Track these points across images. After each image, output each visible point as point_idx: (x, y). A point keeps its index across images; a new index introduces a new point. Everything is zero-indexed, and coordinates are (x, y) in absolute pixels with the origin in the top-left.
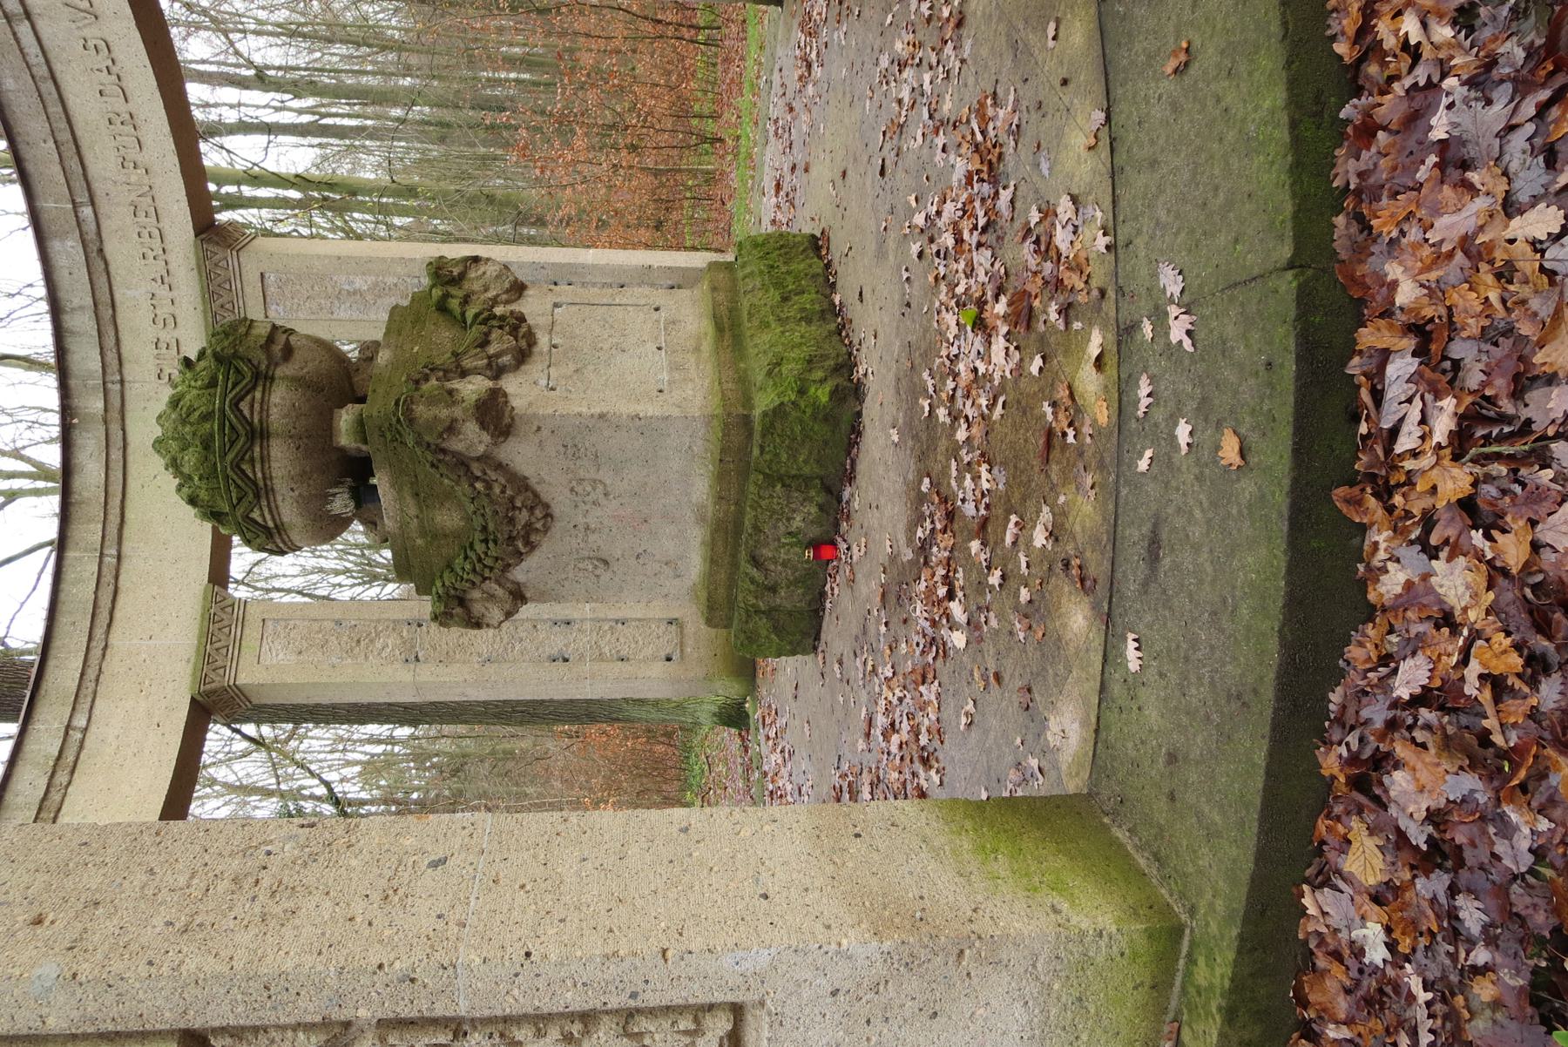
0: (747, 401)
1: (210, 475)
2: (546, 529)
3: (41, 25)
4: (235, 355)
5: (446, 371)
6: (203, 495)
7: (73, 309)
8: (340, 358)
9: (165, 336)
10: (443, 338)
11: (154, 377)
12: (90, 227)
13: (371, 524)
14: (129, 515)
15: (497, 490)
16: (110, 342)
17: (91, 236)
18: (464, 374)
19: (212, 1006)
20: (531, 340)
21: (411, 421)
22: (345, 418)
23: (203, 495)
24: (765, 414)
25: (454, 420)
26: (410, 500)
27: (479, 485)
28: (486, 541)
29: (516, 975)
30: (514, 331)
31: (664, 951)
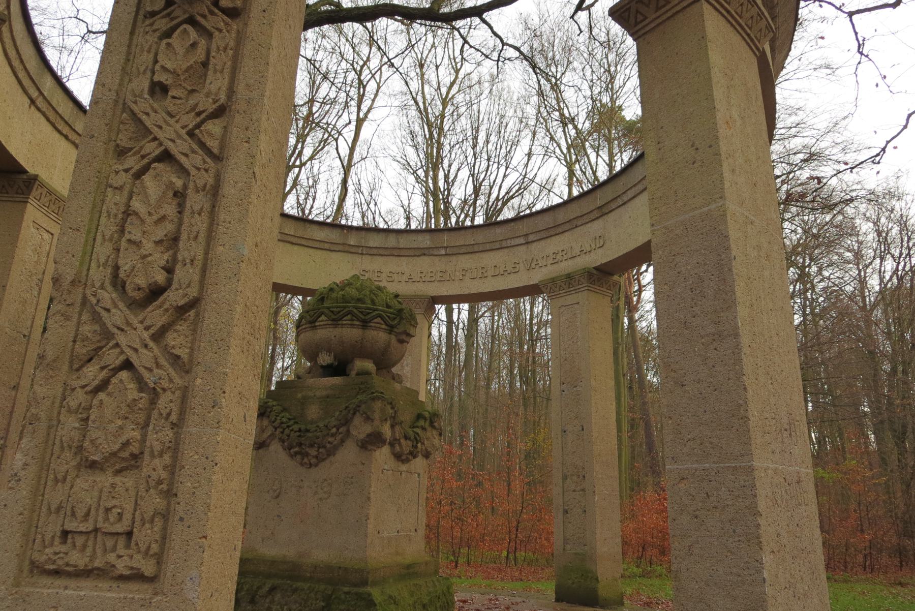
0: (375, 584)
1: (345, 300)
2: (302, 464)
3: (524, 248)
4: (401, 318)
5: (394, 418)
6: (334, 295)
8: (394, 365)
9: (383, 276)
10: (406, 417)
11: (364, 268)
13: (310, 371)
14: (296, 248)
15: (330, 439)
16: (381, 252)
17: (432, 252)
18: (392, 426)
19: (216, 315)
20: (407, 461)
21: (373, 399)
22: (369, 365)
23: (334, 295)
24: (370, 595)
25: (373, 421)
26: (324, 393)
27: (334, 430)
28: (300, 430)
29: (207, 458)
30: (411, 453)
31: (205, 537)
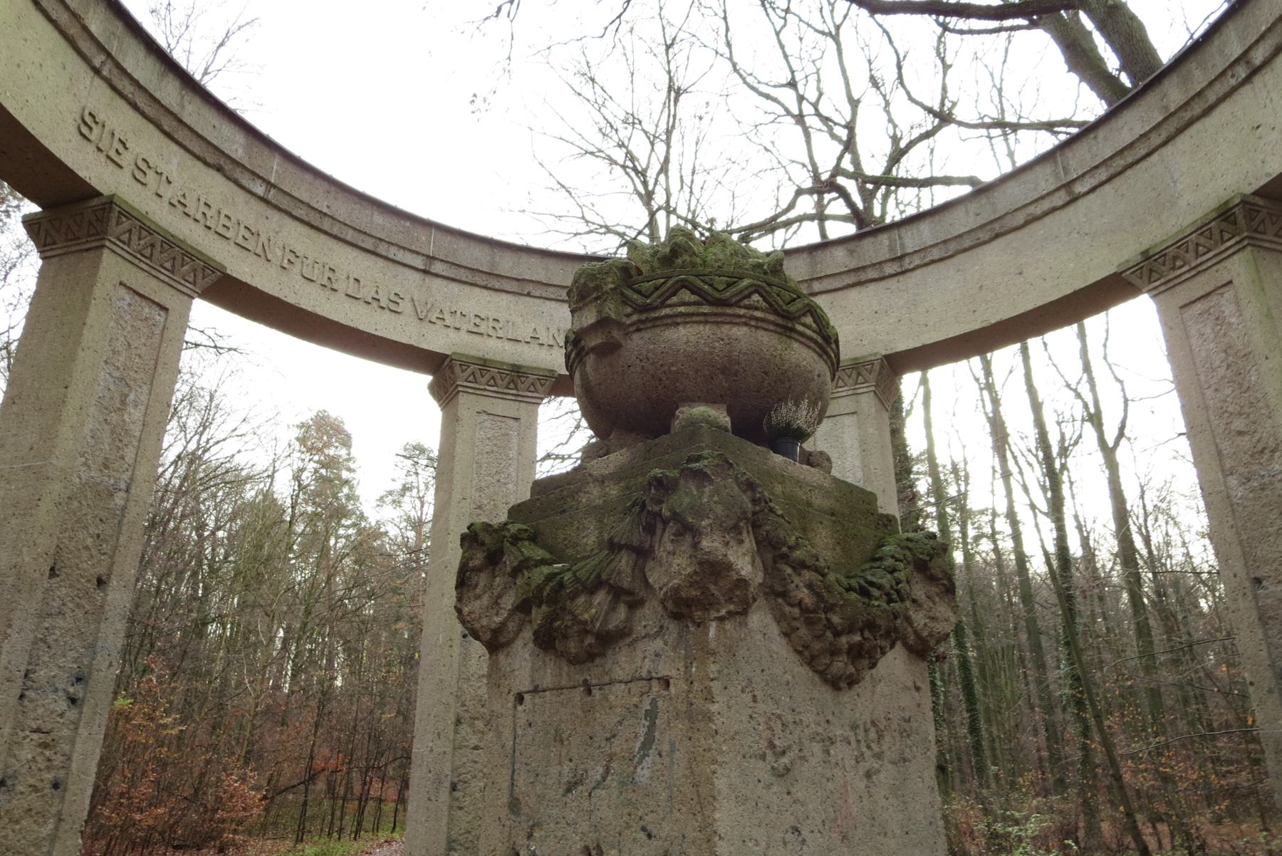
3: (417, 276)
7: (183, 97)
12: (246, 180)
16: (141, 101)
17: (238, 174)
